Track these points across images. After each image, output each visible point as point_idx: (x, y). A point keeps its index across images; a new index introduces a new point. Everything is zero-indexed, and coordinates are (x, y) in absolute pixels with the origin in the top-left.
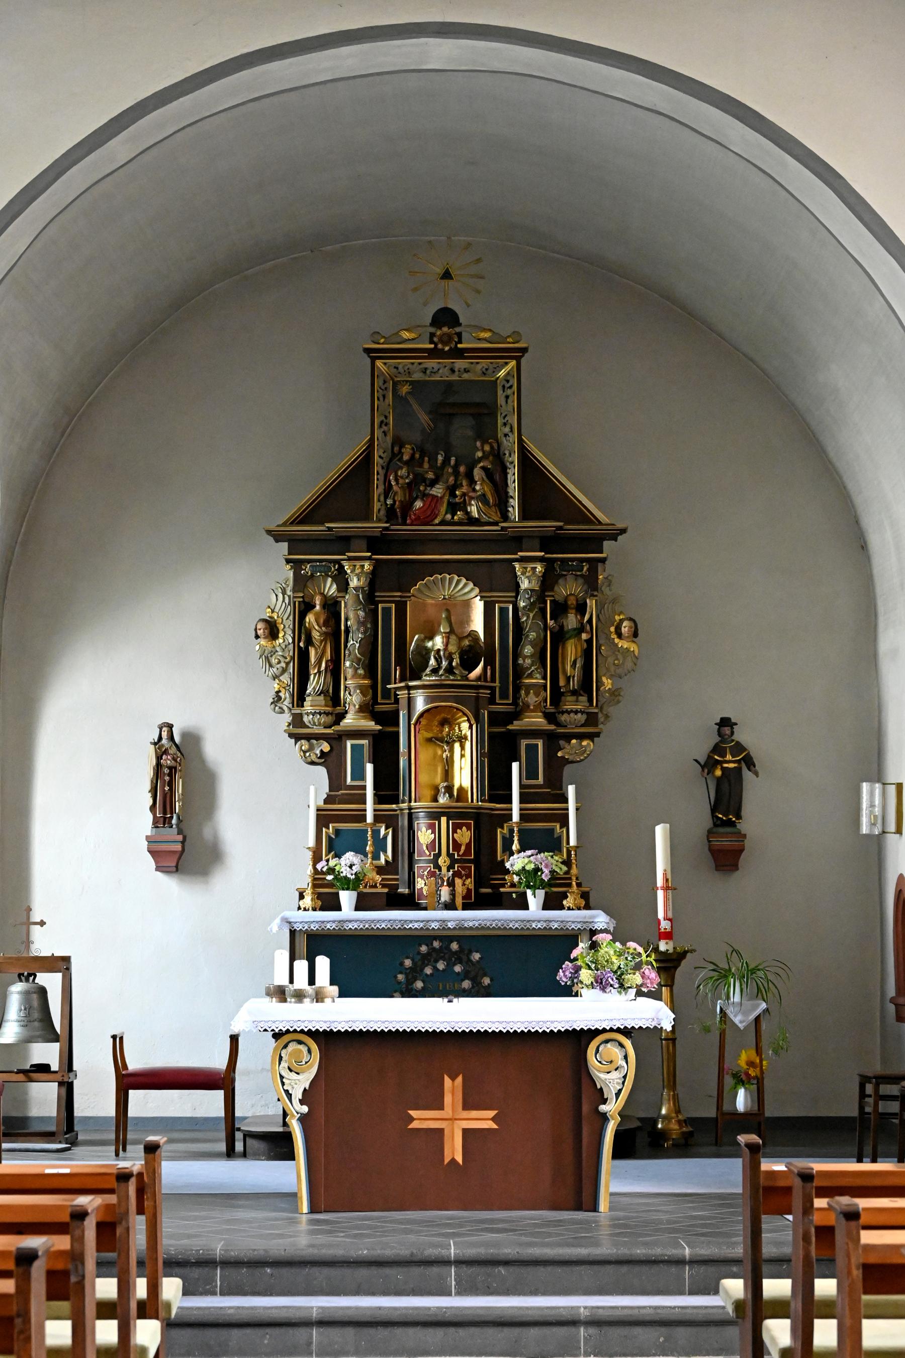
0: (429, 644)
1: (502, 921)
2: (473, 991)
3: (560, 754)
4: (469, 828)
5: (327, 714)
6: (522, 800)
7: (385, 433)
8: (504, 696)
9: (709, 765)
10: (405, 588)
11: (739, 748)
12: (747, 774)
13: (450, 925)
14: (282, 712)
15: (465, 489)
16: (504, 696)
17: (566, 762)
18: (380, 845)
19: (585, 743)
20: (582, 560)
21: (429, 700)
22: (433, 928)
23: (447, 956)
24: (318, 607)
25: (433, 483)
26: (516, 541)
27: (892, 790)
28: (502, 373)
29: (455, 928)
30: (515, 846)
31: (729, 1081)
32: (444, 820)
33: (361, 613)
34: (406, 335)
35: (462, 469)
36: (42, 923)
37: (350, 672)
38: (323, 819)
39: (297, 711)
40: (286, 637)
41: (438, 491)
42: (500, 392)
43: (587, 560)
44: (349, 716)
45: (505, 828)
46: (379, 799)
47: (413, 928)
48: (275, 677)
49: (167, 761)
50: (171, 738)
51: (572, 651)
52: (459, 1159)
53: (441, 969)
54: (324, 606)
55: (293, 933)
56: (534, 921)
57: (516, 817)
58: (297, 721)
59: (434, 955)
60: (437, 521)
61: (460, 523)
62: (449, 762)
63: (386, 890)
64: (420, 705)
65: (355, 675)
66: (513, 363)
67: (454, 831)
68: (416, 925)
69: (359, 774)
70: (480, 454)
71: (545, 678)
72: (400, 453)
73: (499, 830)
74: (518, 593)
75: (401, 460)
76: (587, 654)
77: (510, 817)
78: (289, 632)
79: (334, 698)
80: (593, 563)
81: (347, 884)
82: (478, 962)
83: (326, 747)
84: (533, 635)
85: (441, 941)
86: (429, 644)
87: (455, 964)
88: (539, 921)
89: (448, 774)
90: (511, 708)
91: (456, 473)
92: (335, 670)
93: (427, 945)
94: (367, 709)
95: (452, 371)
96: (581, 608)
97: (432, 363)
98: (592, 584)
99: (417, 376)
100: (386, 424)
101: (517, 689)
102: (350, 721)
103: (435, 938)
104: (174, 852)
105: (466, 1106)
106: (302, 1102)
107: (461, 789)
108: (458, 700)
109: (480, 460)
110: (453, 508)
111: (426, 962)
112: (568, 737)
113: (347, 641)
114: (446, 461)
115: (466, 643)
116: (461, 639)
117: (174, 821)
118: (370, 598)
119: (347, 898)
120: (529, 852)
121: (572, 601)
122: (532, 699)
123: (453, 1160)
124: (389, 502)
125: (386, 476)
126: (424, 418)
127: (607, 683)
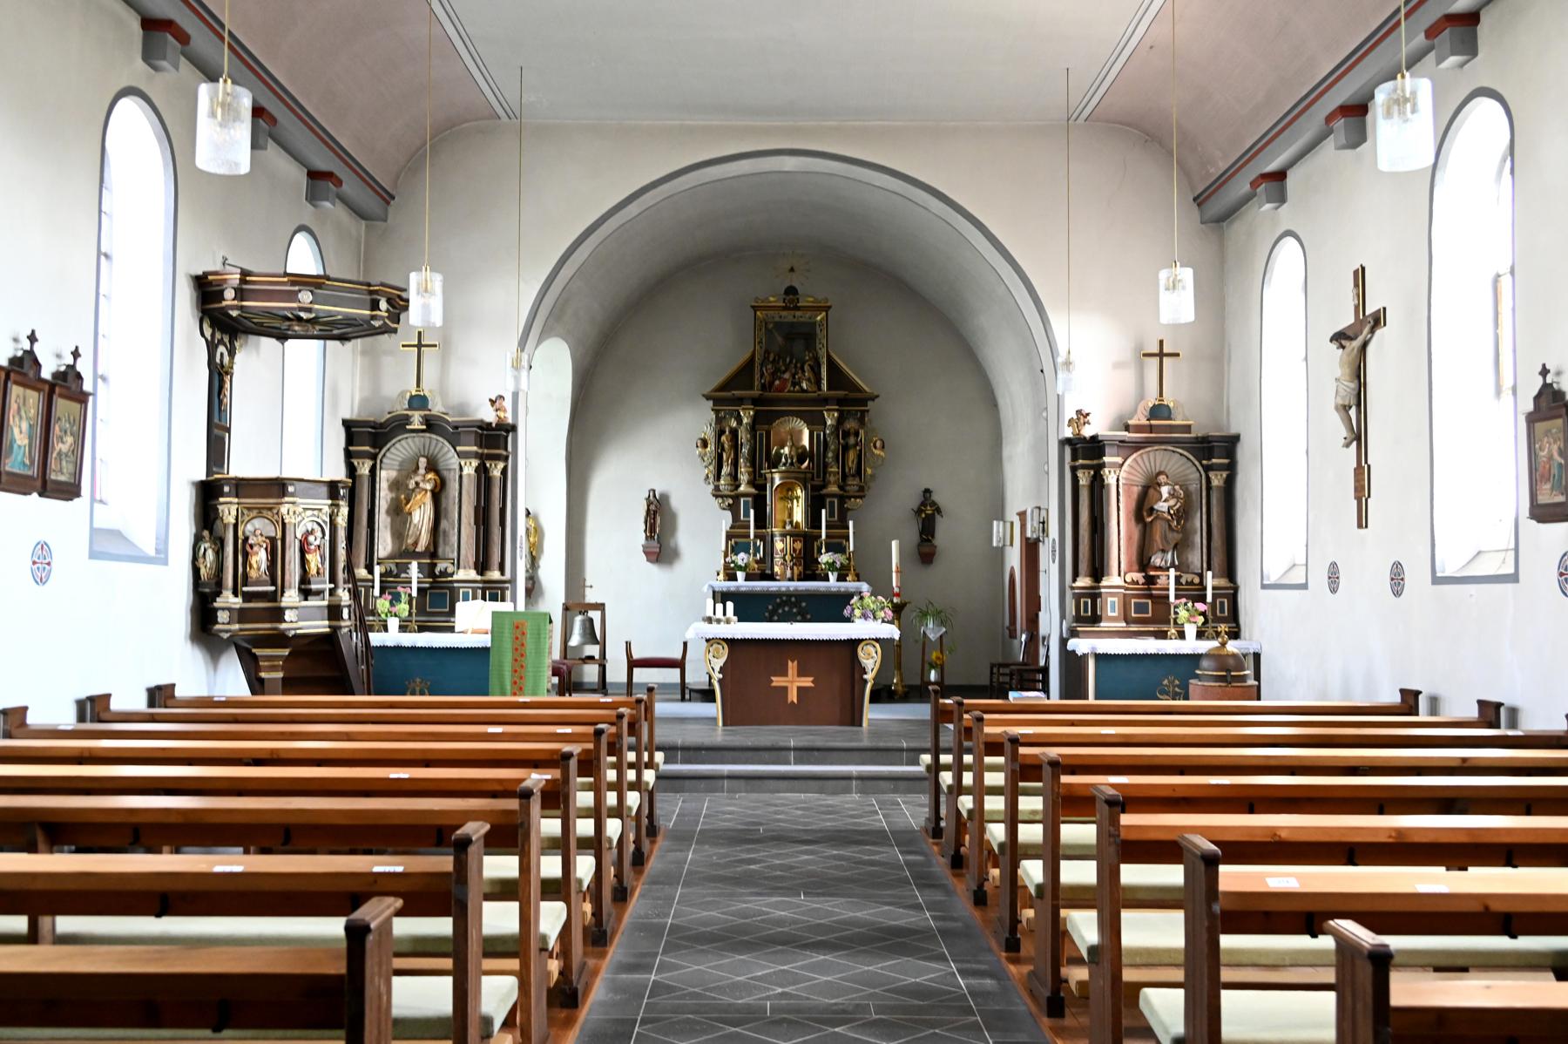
0: (782, 451)
3: (846, 506)
4: (800, 541)
5: (731, 485)
6: (827, 527)
7: (761, 347)
8: (818, 476)
9: (919, 512)
10: (770, 422)
11: (933, 504)
12: (937, 517)
13: (791, 589)
14: (709, 483)
15: (800, 375)
16: (818, 476)
17: (848, 509)
18: (757, 550)
19: (858, 500)
20: (857, 411)
21: (781, 479)
24: (727, 433)
25: (784, 372)
26: (825, 401)
27: (1008, 525)
28: (819, 318)
30: (823, 550)
31: (927, 666)
32: (788, 537)
33: (749, 436)
34: (772, 299)
35: (799, 365)
36: (591, 587)
37: (743, 465)
38: (729, 537)
39: (716, 483)
40: (711, 448)
41: (787, 376)
42: (818, 326)
43: (861, 411)
44: (743, 486)
46: (757, 527)
48: (706, 467)
49: (653, 507)
50: (655, 496)
51: (852, 455)
52: (795, 701)
54: (730, 432)
55: (714, 592)
57: (824, 536)
58: (717, 488)
60: (786, 390)
61: (798, 392)
62: (791, 510)
63: (759, 572)
64: (777, 482)
65: (745, 466)
66: (824, 314)
67: (794, 543)
68: (774, 589)
69: (747, 514)
70: (807, 358)
71: (838, 468)
72: (768, 357)
74: (825, 426)
75: (768, 360)
76: (859, 457)
77: (821, 536)
78: (713, 444)
79: (734, 477)
80: (863, 412)
81: (740, 568)
83: (731, 501)
84: (833, 447)
86: (782, 451)
89: (790, 515)
90: (822, 483)
91: (796, 367)
92: (735, 464)
94: (751, 483)
95: (794, 317)
96: (857, 434)
97: (784, 313)
98: (862, 422)
99: (777, 319)
100: (762, 343)
101: (825, 474)
102: (742, 488)
103: (784, 595)
104: (655, 553)
105: (800, 675)
106: (719, 673)
107: (797, 523)
108: (796, 479)
109: (808, 361)
110: (794, 384)
112: (850, 498)
113: (741, 449)
114: (791, 361)
115: (800, 451)
116: (797, 449)
117: (656, 537)
118: (753, 428)
119: (740, 575)
120: (830, 554)
121: (852, 431)
122: (832, 479)
123: (792, 702)
124: (763, 381)
125: (761, 369)
126: (780, 339)
127: (869, 471)
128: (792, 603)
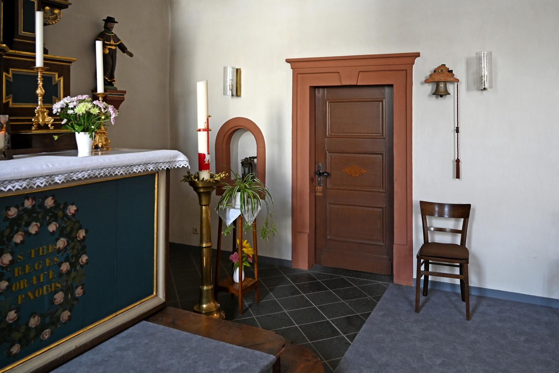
1: (110, 169)
2: (68, 248)
22: (38, 186)
23: (40, 216)
29: (63, 182)
45: (10, 72)
47: (14, 190)
53: (33, 232)
56: (135, 166)
59: (26, 217)
68: (17, 185)
73: (4, 74)
82: (73, 215)
85: (34, 199)
87: (49, 223)
88: (139, 165)
93: (17, 207)
111: (16, 228)
128: (47, 211)
